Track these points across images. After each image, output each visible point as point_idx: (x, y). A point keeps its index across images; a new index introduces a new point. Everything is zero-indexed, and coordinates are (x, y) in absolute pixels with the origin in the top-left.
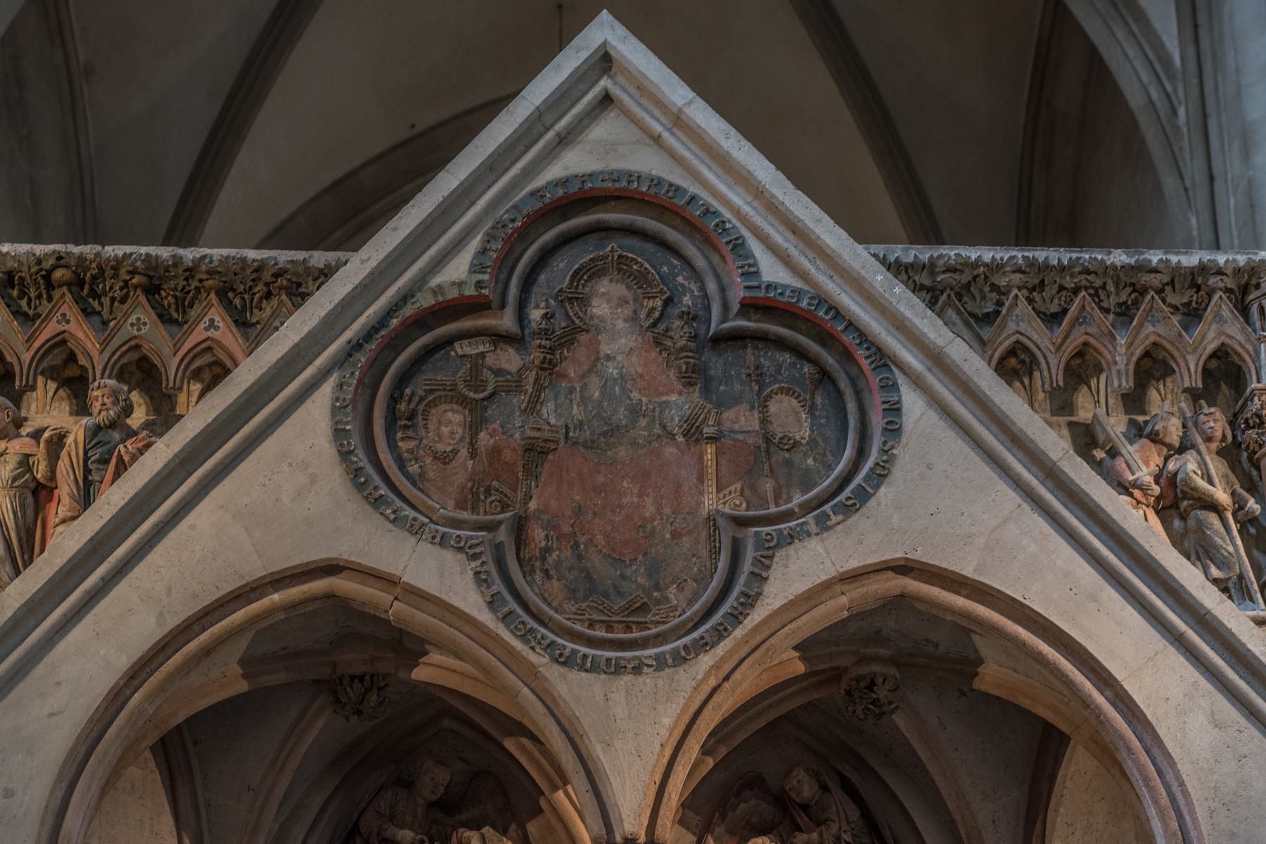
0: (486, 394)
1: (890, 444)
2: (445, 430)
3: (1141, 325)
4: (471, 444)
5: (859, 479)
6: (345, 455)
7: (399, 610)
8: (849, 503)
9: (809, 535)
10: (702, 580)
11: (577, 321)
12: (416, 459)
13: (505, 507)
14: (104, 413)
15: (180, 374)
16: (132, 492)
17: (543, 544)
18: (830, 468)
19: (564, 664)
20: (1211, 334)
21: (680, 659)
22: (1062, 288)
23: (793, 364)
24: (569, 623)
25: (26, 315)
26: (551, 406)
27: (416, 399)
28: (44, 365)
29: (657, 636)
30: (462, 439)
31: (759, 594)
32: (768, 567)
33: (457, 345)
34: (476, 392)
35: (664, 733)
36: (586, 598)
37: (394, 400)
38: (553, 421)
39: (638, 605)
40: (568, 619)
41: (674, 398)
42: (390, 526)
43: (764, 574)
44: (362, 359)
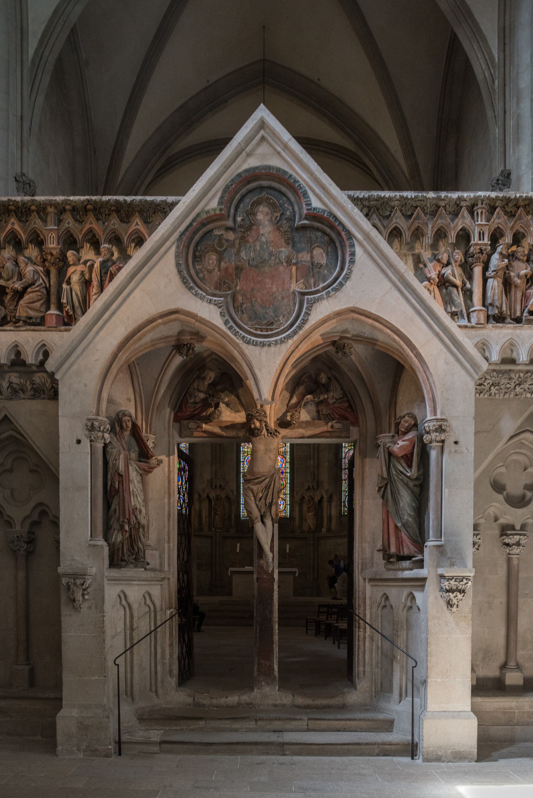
0: (223, 249)
2: (211, 262)
3: (437, 220)
4: (219, 266)
6: (180, 272)
9: (324, 299)
11: (252, 222)
13: (230, 289)
16: (115, 287)
18: (332, 274)
20: (460, 223)
21: (282, 341)
23: (322, 236)
25: (79, 221)
26: (244, 252)
28: (86, 238)
29: (276, 333)
30: (216, 265)
31: (307, 319)
32: (310, 310)
33: (214, 231)
34: (220, 248)
35: (277, 366)
36: (254, 320)
37: (195, 252)
38: (244, 258)
41: (283, 249)
42: (194, 296)
43: (309, 312)
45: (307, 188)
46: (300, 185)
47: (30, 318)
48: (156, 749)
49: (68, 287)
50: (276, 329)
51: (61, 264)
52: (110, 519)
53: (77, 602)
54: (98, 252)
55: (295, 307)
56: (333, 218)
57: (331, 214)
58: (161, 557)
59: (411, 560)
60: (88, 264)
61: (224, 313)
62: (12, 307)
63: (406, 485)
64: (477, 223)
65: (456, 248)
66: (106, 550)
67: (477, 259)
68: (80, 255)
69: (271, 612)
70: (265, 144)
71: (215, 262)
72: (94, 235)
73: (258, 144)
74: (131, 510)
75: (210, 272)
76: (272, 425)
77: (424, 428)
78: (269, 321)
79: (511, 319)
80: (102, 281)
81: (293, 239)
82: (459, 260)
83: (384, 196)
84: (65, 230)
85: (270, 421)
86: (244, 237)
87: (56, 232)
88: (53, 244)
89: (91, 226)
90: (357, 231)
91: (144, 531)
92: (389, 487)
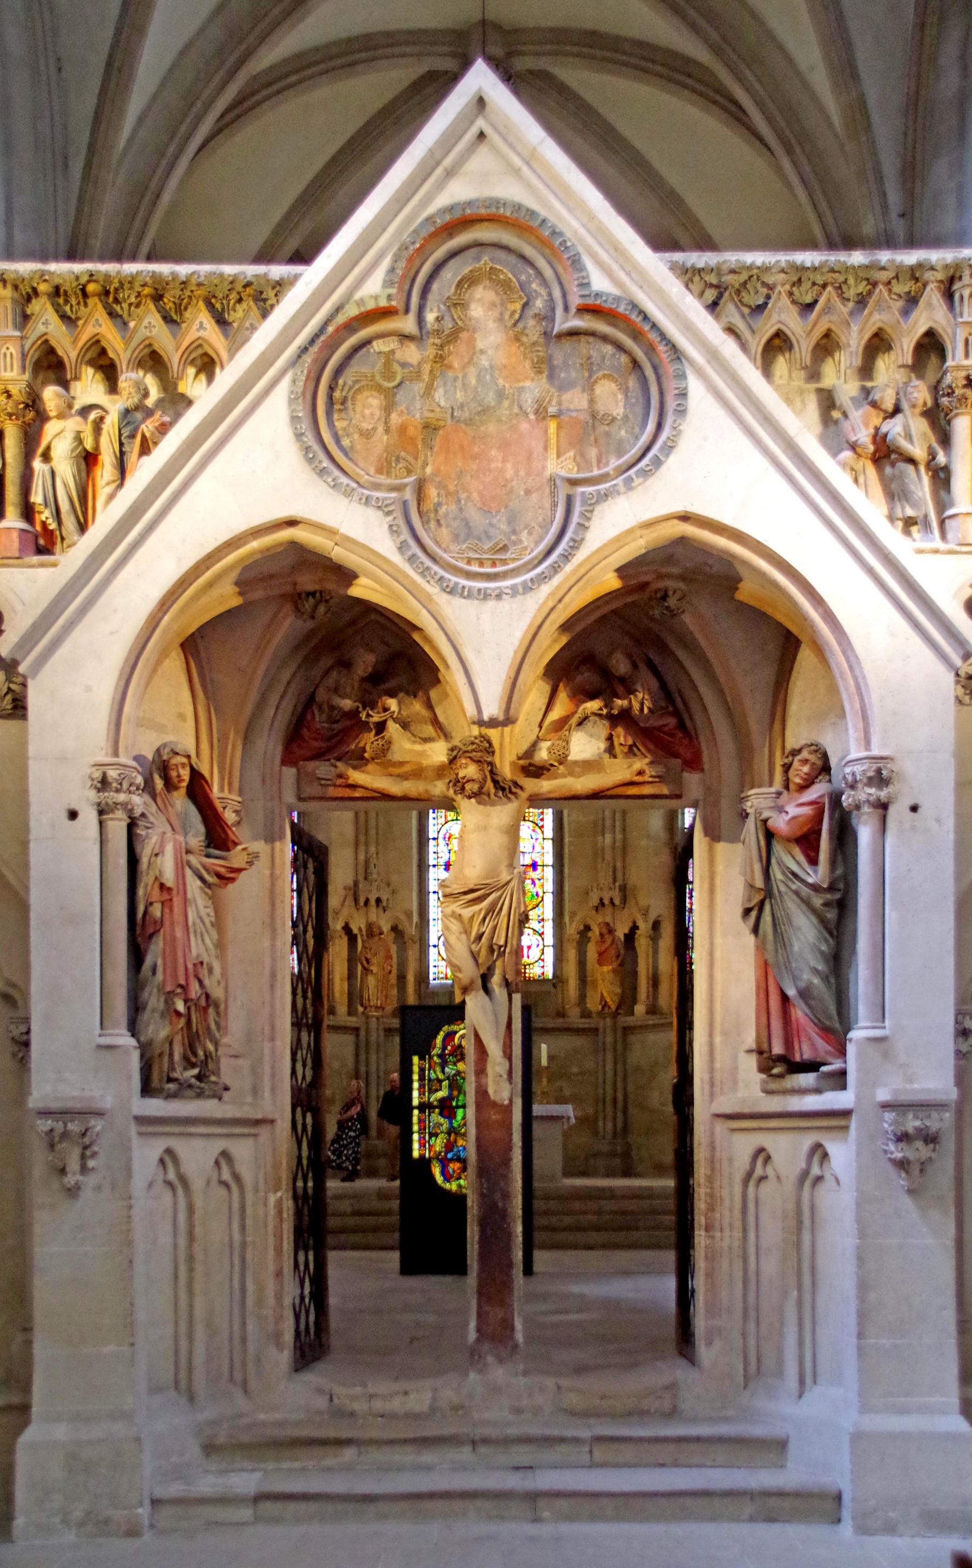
0: (395, 383)
1: (678, 421)
2: (367, 412)
3: (871, 314)
4: (386, 423)
5: (655, 450)
6: (299, 436)
7: (338, 554)
8: (647, 469)
9: (618, 493)
10: (545, 527)
11: (460, 323)
12: (348, 435)
13: (409, 472)
14: (130, 400)
15: (181, 368)
17: (436, 500)
19: (450, 593)
20: (922, 320)
21: (528, 588)
22: (814, 284)
23: (613, 355)
24: (453, 561)
25: (69, 318)
27: (347, 388)
29: (513, 570)
30: (379, 419)
31: (583, 539)
32: (589, 519)
33: (375, 343)
34: (389, 381)
36: (464, 542)
37: (331, 389)
38: (443, 404)
39: (501, 546)
40: (453, 557)
41: (528, 384)
42: (330, 490)
43: (586, 524)
44: (308, 359)
45: (581, 249)
46: (565, 241)
48: (246, 1513)
50: (514, 560)
51: (31, 415)
52: (142, 989)
53: (69, 1175)
54: (112, 387)
55: (555, 511)
56: (638, 316)
57: (634, 306)
58: (255, 1071)
59: (817, 1070)
60: (93, 415)
61: (398, 526)
63: (807, 903)
64: (960, 320)
65: (913, 375)
66: (136, 1055)
67: (959, 400)
68: (72, 393)
69: (506, 1196)
70: (483, 150)
71: (378, 413)
72: (103, 352)
73: (471, 150)
74: (190, 966)
75: (367, 435)
76: (506, 771)
77: (845, 778)
78: (497, 544)
80: (122, 453)
81: (549, 360)
82: (921, 402)
83: (753, 262)
84: (38, 339)
85: (501, 761)
86: (441, 356)
87: (18, 343)
88: (12, 370)
89: (97, 330)
90: (692, 344)
91: (218, 1013)
92: (767, 908)
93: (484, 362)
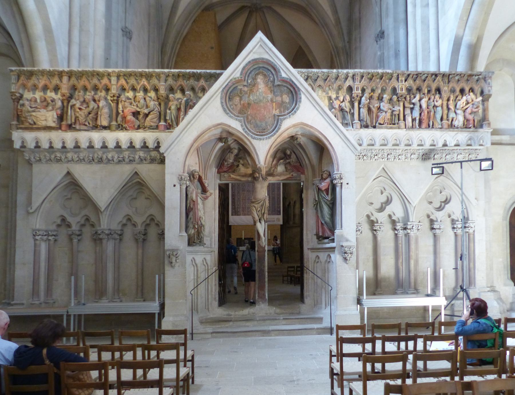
4: (240, 103)
5: (295, 109)
6: (222, 106)
13: (245, 113)
41: (269, 95)
47: (152, 126)
49: (170, 111)
51: (166, 100)
60: (180, 100)
62: (143, 121)
71: (238, 101)
75: (236, 105)
79: (371, 126)
93: (260, 91)
